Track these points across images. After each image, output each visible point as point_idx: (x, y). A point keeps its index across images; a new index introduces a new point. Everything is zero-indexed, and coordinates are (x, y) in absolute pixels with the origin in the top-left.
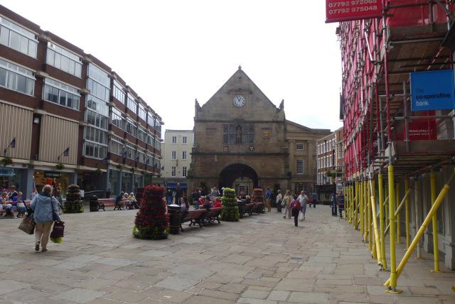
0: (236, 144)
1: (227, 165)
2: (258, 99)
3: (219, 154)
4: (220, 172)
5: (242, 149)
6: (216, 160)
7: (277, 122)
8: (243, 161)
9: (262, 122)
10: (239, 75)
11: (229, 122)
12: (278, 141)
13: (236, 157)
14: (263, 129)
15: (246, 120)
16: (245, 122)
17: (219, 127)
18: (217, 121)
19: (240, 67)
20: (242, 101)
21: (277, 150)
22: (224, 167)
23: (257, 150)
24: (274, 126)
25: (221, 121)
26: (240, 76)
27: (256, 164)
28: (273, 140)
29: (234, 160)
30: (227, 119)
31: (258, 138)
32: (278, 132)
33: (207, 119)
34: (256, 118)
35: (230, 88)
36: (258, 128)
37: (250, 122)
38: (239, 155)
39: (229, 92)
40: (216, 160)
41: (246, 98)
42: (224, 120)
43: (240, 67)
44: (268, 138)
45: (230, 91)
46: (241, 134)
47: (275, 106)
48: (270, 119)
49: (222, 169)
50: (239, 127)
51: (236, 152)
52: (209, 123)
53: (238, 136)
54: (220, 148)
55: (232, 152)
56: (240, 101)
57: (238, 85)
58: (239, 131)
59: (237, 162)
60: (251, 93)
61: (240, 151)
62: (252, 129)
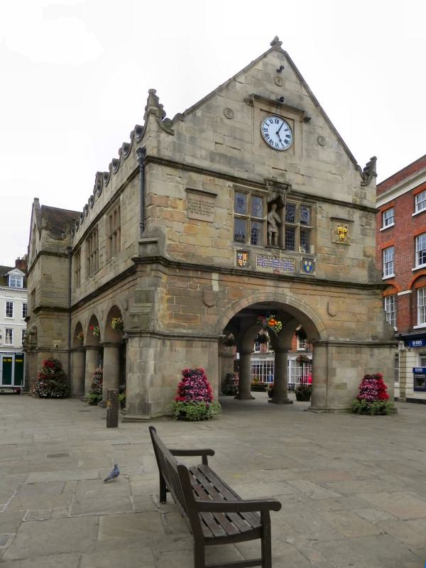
0: (268, 247)
1: (245, 304)
4: (225, 322)
6: (216, 288)
8: (289, 295)
10: (276, 61)
14: (333, 219)
15: (295, 187)
16: (294, 194)
17: (225, 191)
19: (276, 44)
20: (283, 134)
21: (362, 276)
22: (238, 309)
23: (319, 273)
24: (357, 215)
27: (314, 305)
28: (354, 252)
29: (264, 293)
31: (322, 239)
32: (364, 234)
35: (252, 90)
39: (251, 101)
40: (216, 288)
41: (293, 131)
42: (237, 174)
43: (276, 44)
44: (346, 245)
45: (257, 98)
46: (279, 225)
47: (357, 168)
48: (349, 199)
49: (231, 315)
51: (270, 270)
52: (194, 175)
53: (274, 229)
54: (226, 255)
55: (260, 269)
56: (275, 130)
57: (274, 92)
58: (273, 213)
59: (271, 299)
60: (307, 120)
61: (282, 272)
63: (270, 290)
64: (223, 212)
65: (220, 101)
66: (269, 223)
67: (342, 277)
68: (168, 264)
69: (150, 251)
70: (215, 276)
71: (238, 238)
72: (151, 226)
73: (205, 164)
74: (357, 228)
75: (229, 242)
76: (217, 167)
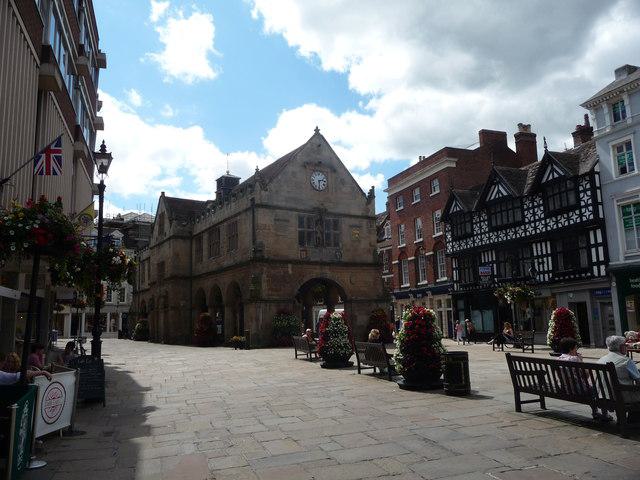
0: (316, 246)
1: (305, 280)
2: (343, 182)
3: (295, 262)
5: (327, 254)
6: (290, 272)
7: (368, 218)
8: (328, 273)
9: (351, 216)
11: (304, 211)
12: (370, 244)
13: (318, 267)
14: (352, 226)
16: (330, 214)
18: (291, 209)
19: (317, 130)
20: (322, 183)
21: (369, 259)
23: (345, 259)
24: (365, 222)
25: (296, 210)
26: (318, 142)
27: (343, 278)
28: (364, 244)
29: (316, 272)
30: (302, 207)
31: (346, 239)
32: (370, 232)
33: (275, 203)
34: (340, 209)
35: (306, 159)
36: (345, 223)
37: (335, 215)
38: (323, 264)
39: (305, 165)
40: (290, 272)
43: (317, 130)
44: (359, 241)
46: (322, 233)
48: (359, 213)
50: (320, 221)
51: (317, 259)
53: (319, 235)
54: (295, 252)
55: (312, 260)
56: (318, 179)
60: (335, 171)
62: (336, 225)
63: (317, 271)
64: (293, 229)
65: (290, 169)
66: (317, 233)
67: (358, 260)
68: (267, 261)
69: (258, 255)
70: (290, 266)
71: (301, 243)
72: (258, 240)
73: (283, 204)
74: (365, 229)
75: (296, 245)
76: (289, 205)
